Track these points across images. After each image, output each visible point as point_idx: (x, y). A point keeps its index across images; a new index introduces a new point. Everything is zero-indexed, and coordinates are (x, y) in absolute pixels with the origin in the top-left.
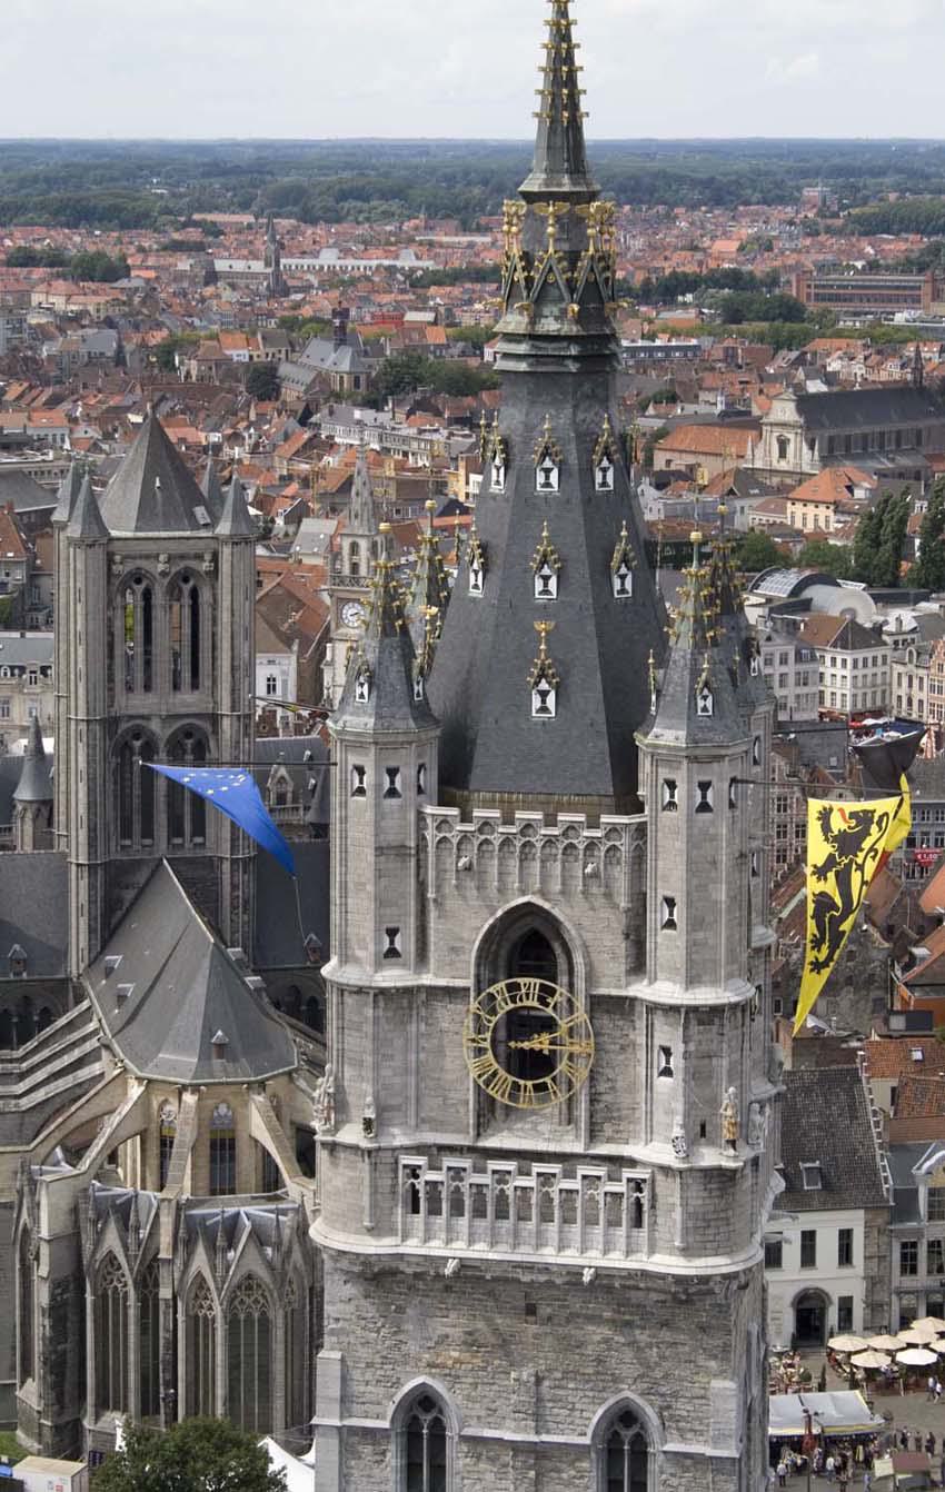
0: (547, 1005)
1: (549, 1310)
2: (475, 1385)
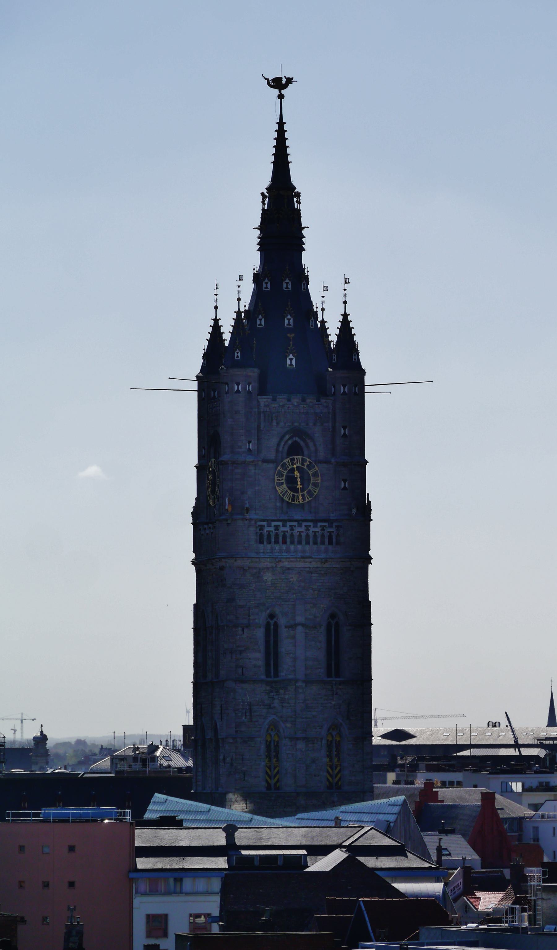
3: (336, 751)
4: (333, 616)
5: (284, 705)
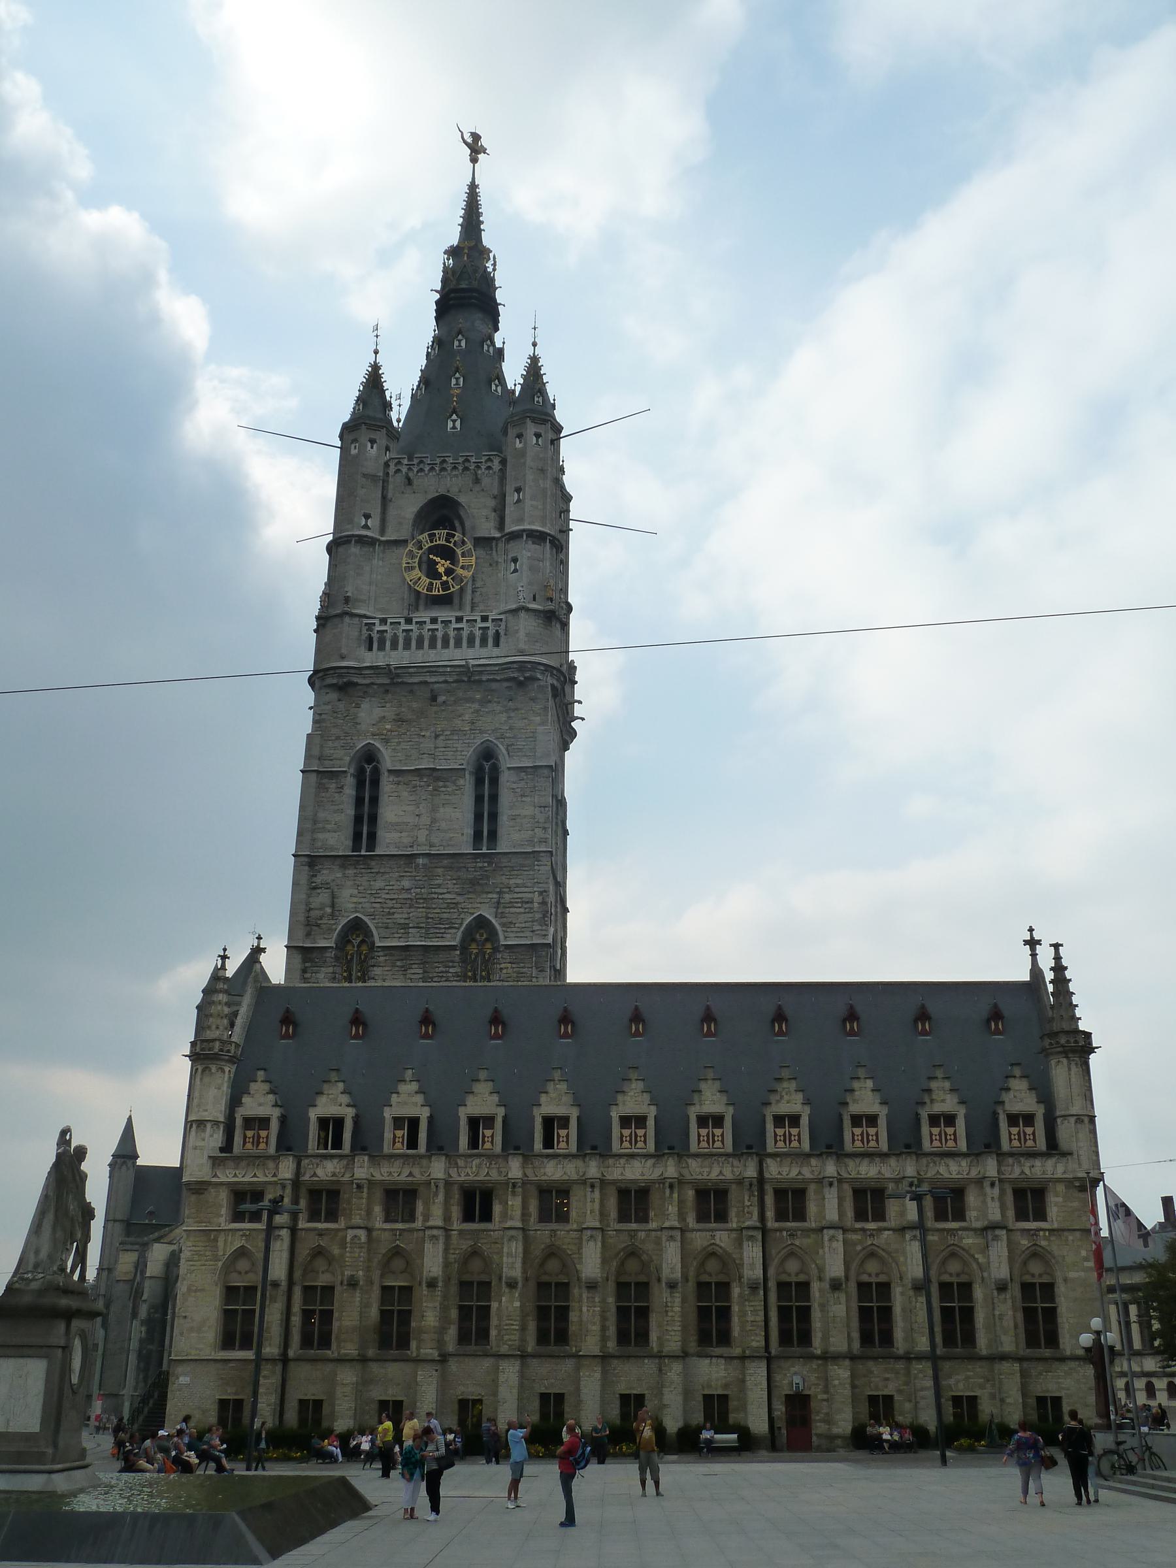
0: (450, 542)
1: (444, 698)
2: (399, 743)
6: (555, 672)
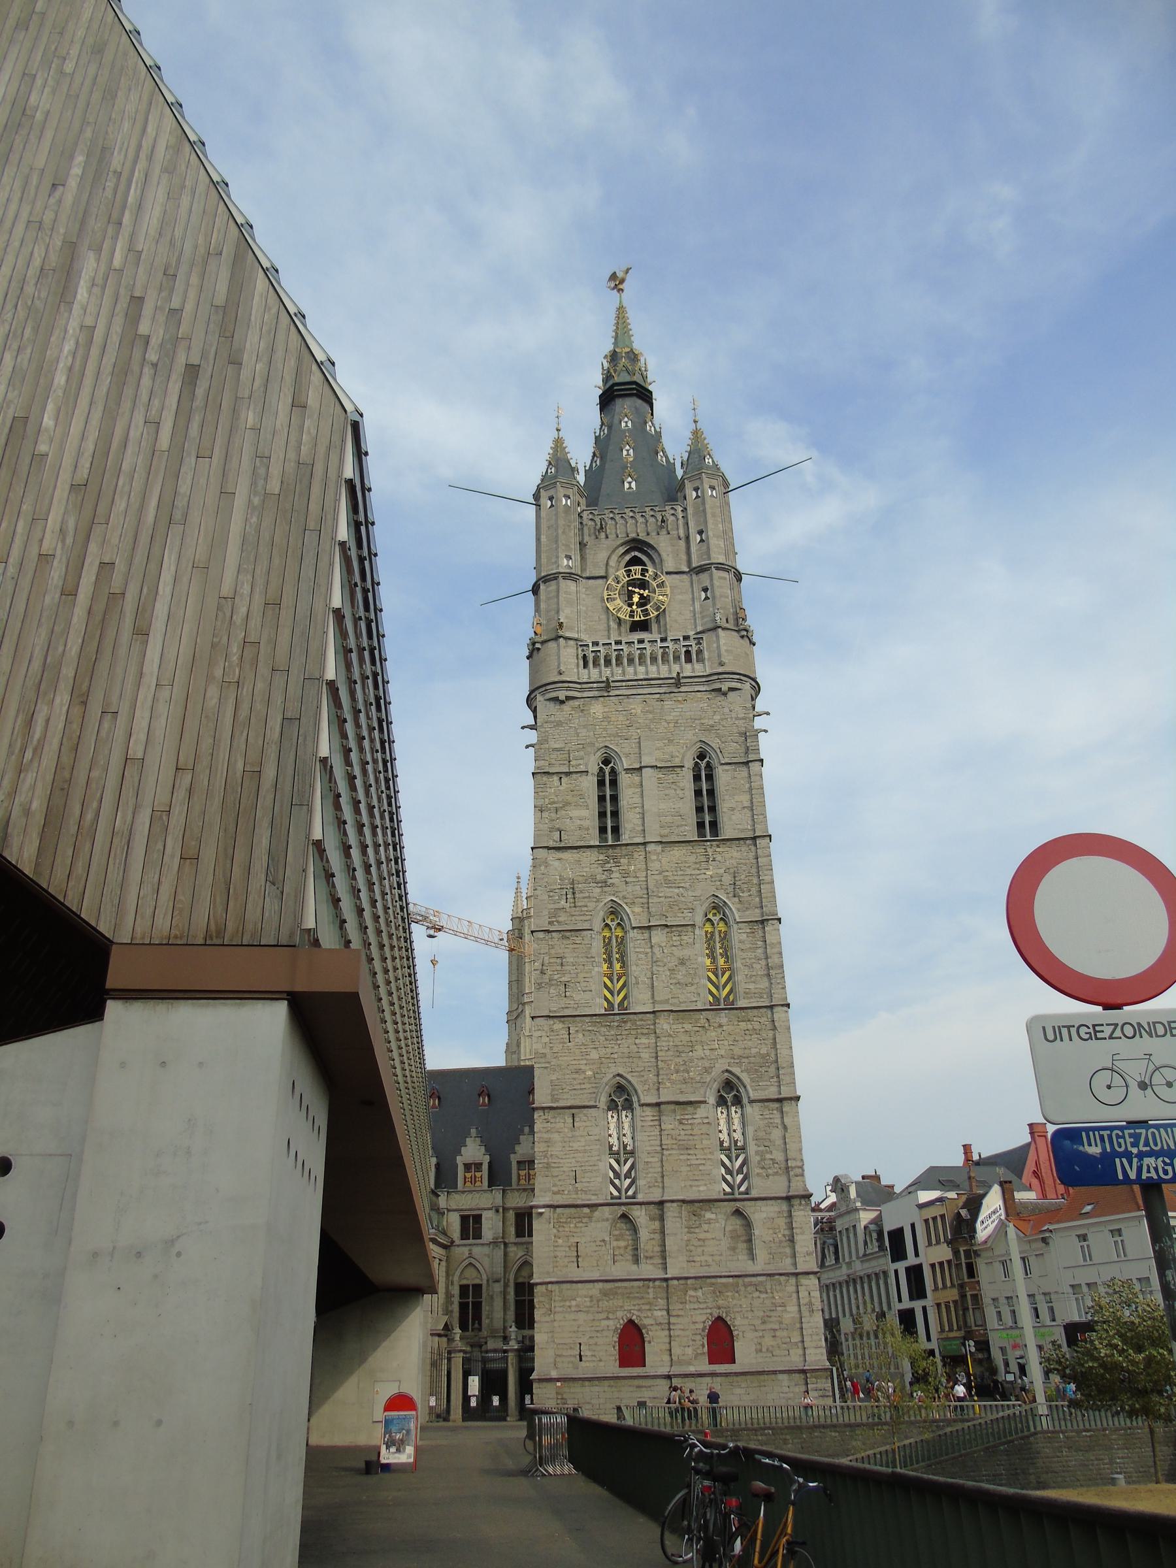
3: (721, 948)
4: (702, 756)
5: (628, 880)
6: (754, 683)
